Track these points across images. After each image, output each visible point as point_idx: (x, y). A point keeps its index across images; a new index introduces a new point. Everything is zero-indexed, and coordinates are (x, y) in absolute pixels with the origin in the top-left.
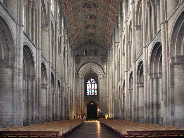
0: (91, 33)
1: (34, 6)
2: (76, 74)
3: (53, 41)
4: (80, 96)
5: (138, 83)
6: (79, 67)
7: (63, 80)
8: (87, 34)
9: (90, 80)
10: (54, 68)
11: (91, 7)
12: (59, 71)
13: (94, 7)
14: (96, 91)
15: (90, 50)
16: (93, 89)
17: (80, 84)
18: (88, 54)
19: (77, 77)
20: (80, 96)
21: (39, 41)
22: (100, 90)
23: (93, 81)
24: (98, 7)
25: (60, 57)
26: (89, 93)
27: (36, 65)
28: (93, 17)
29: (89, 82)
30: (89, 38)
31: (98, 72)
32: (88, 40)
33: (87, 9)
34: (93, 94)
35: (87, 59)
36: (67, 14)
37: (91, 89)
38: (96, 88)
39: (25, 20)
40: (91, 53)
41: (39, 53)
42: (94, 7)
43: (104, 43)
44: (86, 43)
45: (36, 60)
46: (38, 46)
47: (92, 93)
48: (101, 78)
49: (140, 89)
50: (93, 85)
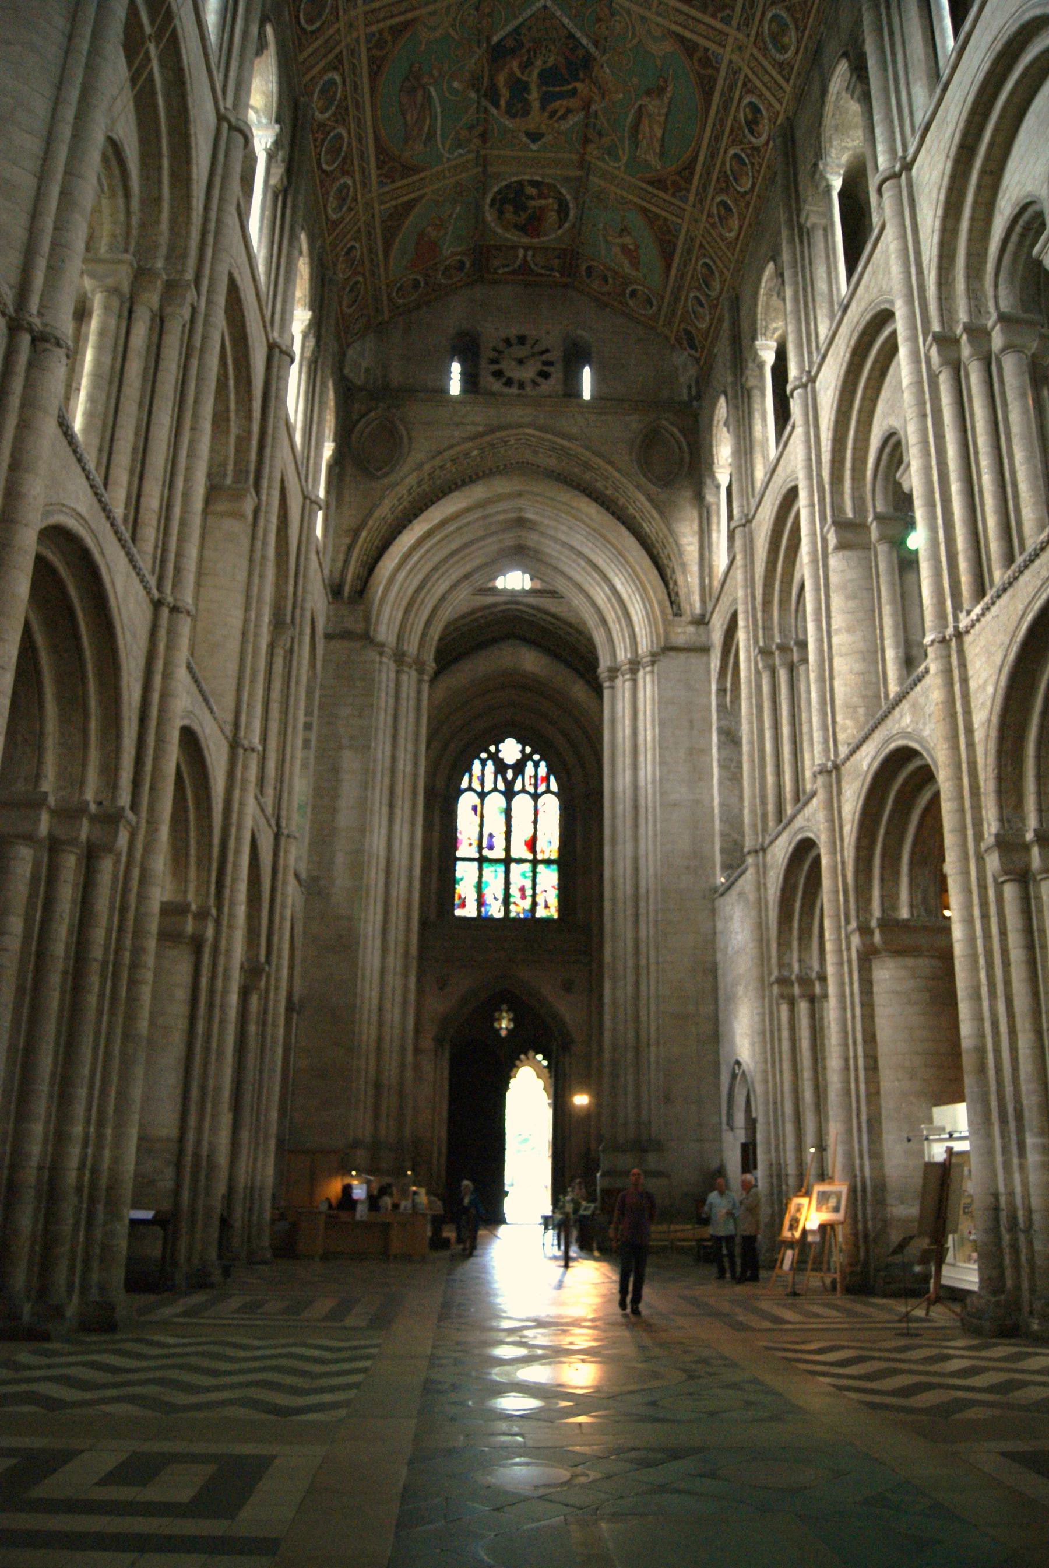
2: (335, 591)
4: (375, 877)
6: (376, 514)
8: (498, 54)
9: (495, 757)
14: (549, 878)
15: (522, 340)
16: (519, 850)
17: (383, 719)
18: (496, 386)
19: (347, 635)
20: (375, 877)
22: (623, 807)
23: (519, 768)
26: (481, 902)
31: (601, 596)
34: (519, 908)
35: (471, 439)
37: (499, 853)
38: (550, 845)
40: (528, 373)
47: (506, 902)
48: (635, 665)
50: (522, 804)
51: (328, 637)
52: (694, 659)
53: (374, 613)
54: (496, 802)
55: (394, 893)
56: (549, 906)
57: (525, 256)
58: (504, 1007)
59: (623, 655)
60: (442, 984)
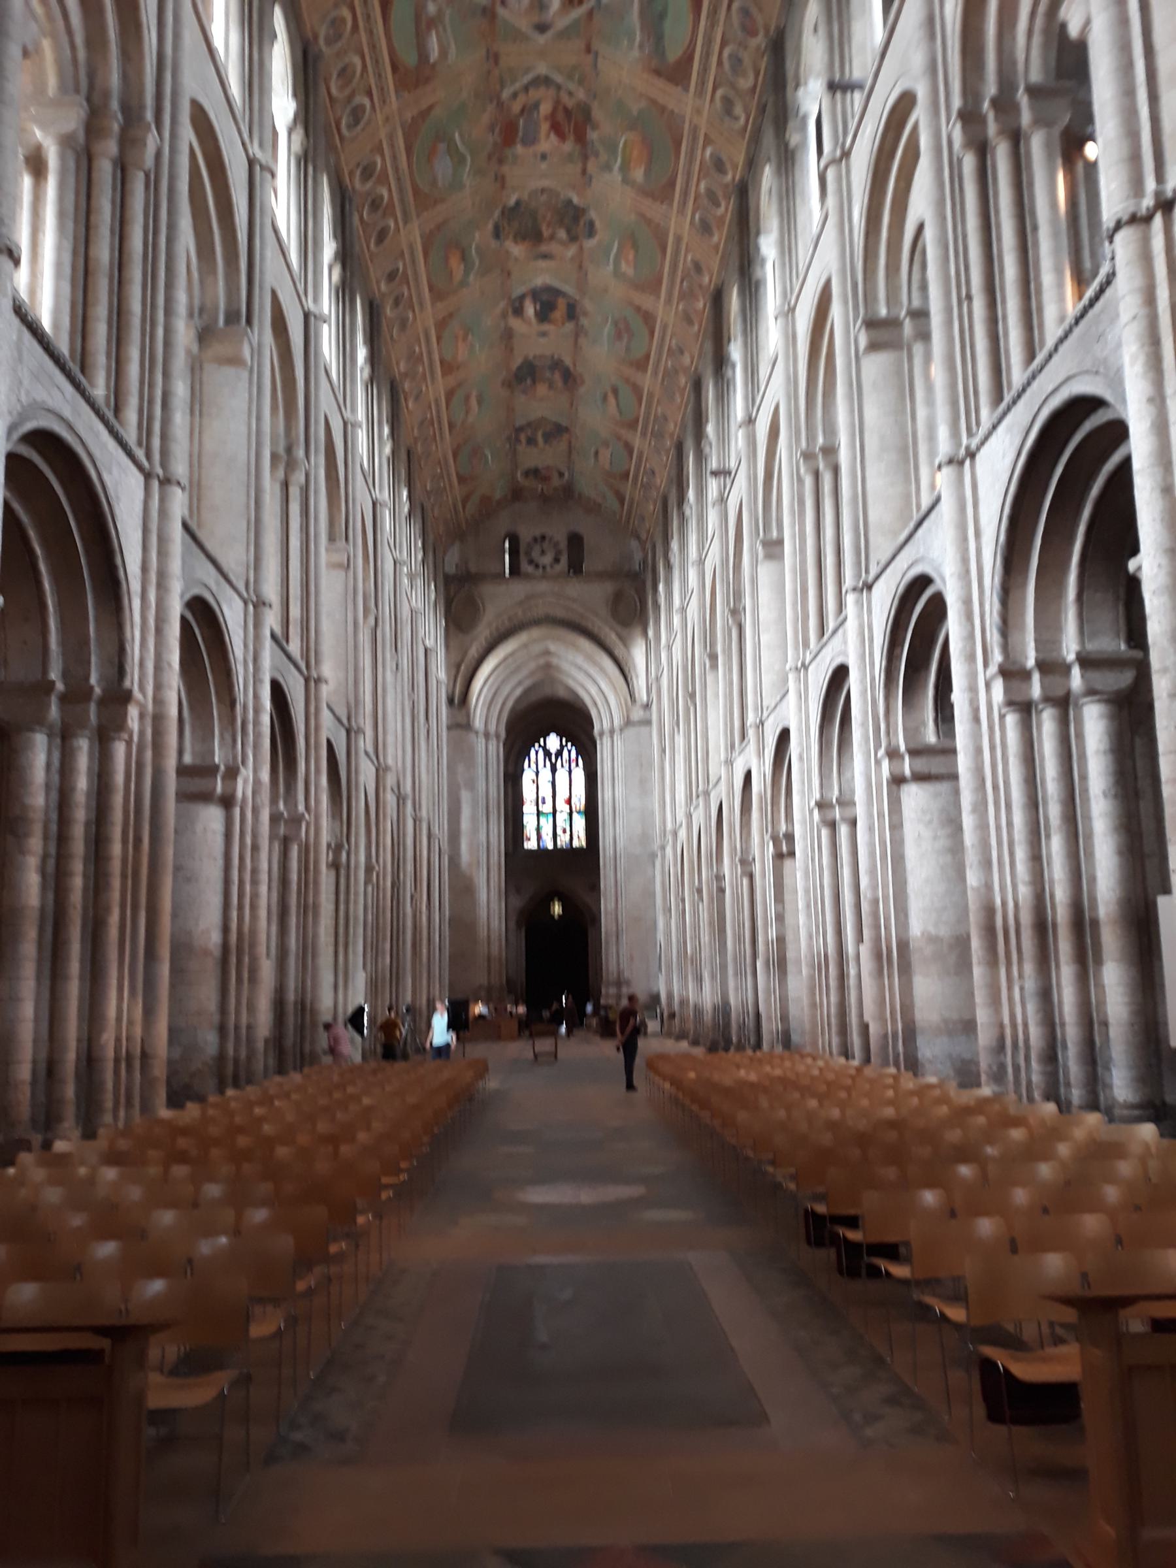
0: (542, 421)
1: (129, 140)
2: (450, 701)
3: (289, 450)
5: (893, 754)
7: (365, 743)
8: (519, 430)
10: (294, 647)
11: (546, 233)
12: (328, 669)
13: (562, 234)
14: (580, 823)
15: (543, 538)
17: (481, 771)
21: (166, 421)
23: (559, 753)
24: (591, 230)
25: (341, 574)
26: (539, 837)
27: (136, 603)
28: (561, 303)
29: (536, 754)
30: (532, 457)
31: (593, 690)
32: (527, 474)
33: (517, 250)
34: (563, 840)
36: (392, 276)
39: (59, 249)
41: (163, 513)
42: (568, 231)
43: (628, 489)
44: (517, 494)
45: (145, 569)
46: (157, 457)
48: (612, 732)
49: (914, 797)
50: (562, 774)
51: (449, 728)
52: (644, 730)
53: (472, 711)
54: (546, 773)
55: (492, 861)
56: (580, 841)
57: (542, 489)
58: (556, 899)
59: (606, 725)
60: (518, 891)
